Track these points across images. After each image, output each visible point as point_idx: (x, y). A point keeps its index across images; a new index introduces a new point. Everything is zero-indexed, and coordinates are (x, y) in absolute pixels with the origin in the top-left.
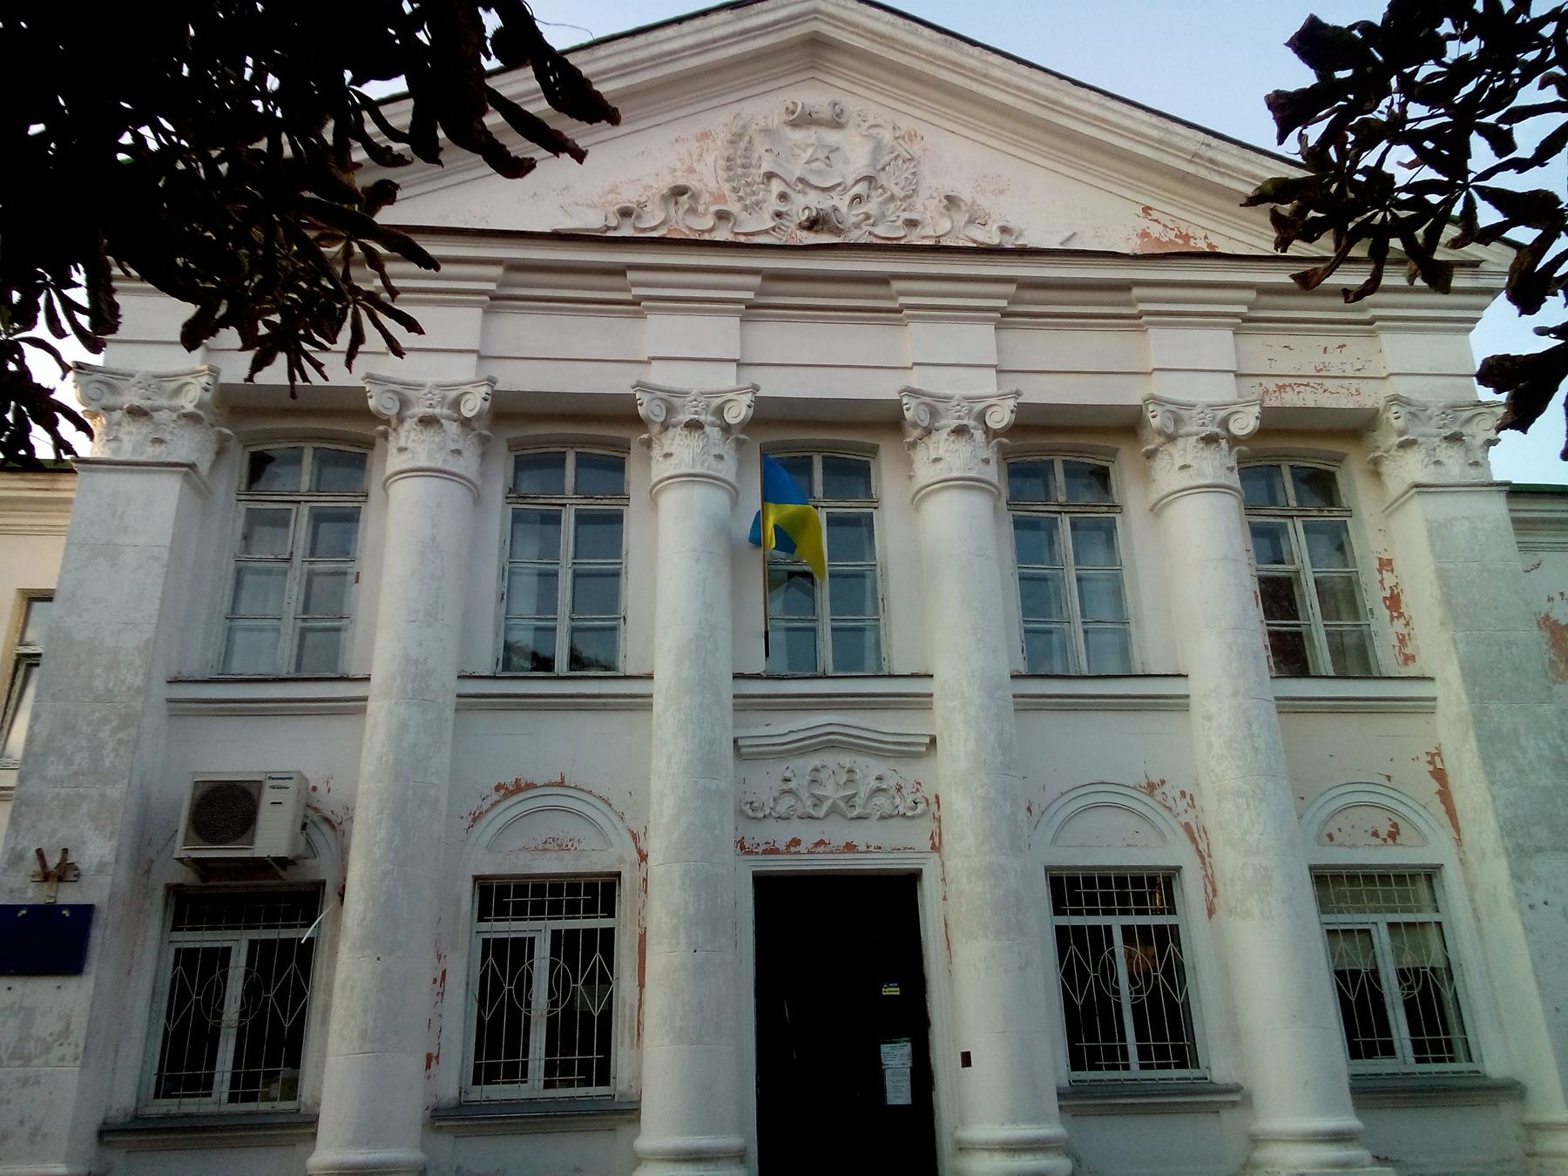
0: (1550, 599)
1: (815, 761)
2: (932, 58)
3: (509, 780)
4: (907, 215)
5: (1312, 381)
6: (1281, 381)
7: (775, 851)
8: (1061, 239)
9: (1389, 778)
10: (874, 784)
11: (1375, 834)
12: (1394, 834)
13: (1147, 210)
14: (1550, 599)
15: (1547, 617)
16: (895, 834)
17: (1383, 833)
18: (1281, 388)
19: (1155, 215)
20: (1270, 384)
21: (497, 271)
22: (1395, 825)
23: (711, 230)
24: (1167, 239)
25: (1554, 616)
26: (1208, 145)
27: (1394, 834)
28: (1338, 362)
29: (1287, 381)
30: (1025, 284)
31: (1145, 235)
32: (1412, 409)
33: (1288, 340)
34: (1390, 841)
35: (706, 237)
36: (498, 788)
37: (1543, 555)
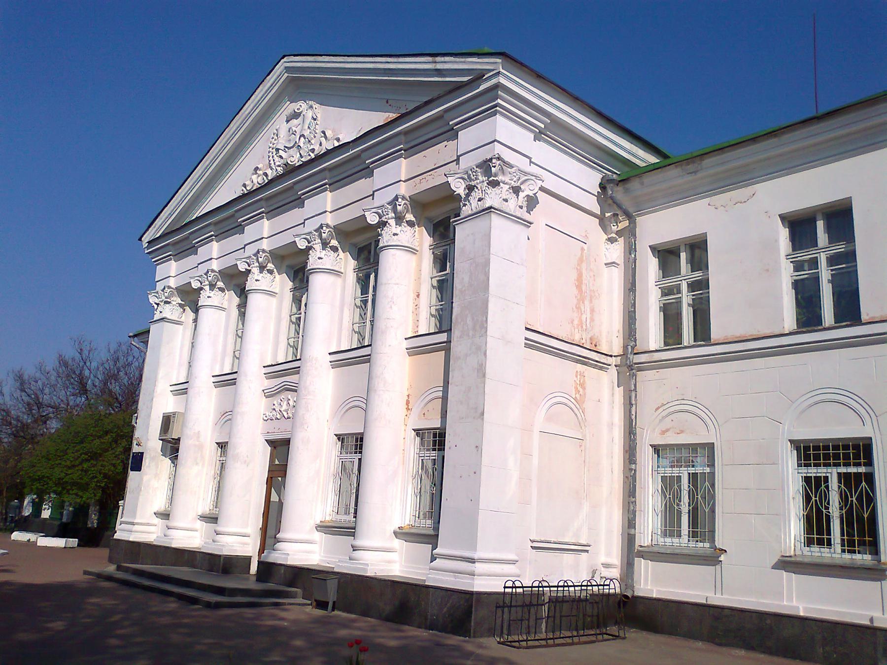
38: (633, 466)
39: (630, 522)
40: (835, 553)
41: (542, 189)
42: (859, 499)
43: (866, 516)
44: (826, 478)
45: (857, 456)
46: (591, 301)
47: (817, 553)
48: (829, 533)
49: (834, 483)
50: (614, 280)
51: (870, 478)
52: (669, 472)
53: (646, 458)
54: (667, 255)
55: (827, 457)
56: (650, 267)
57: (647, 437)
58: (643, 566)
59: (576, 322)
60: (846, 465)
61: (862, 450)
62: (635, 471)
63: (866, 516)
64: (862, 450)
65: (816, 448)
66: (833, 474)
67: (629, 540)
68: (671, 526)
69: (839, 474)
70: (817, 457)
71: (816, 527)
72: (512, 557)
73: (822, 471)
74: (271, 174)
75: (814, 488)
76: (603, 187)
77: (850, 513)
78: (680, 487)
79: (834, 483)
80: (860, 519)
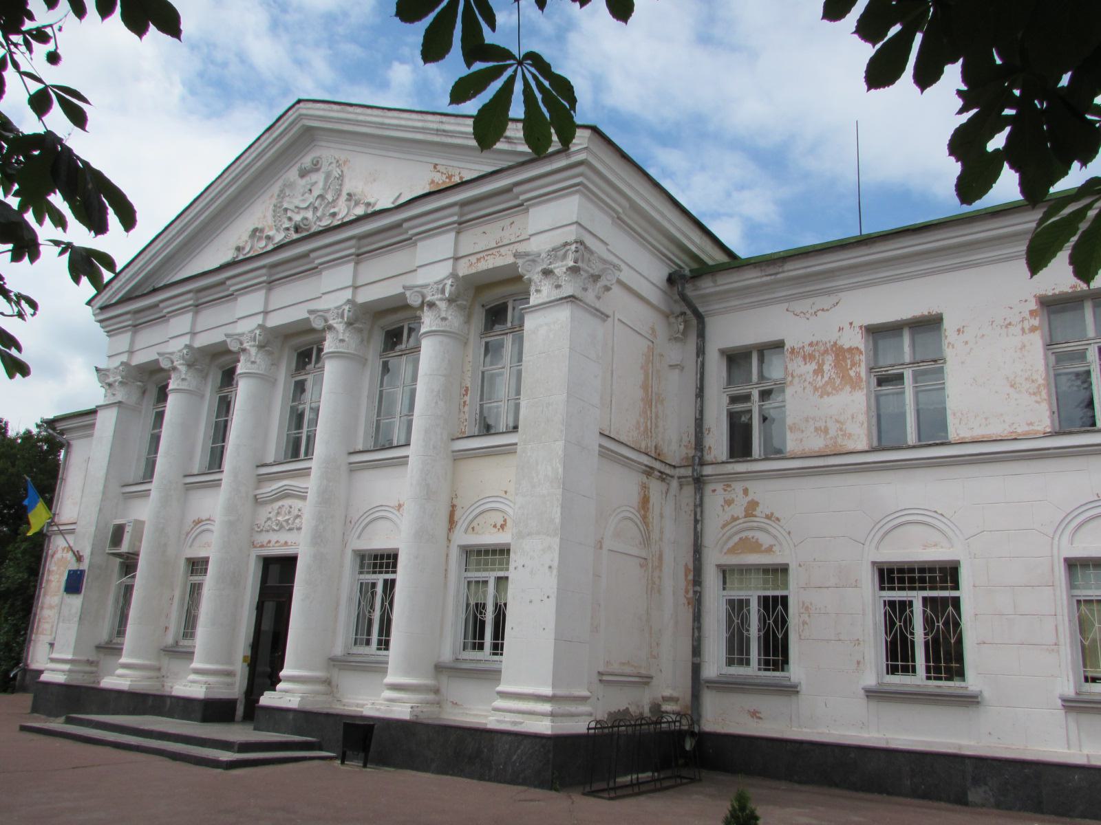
0: (841, 329)
1: (280, 503)
2: (339, 121)
3: (196, 518)
4: (332, 211)
5: (494, 251)
6: (478, 256)
7: (262, 546)
8: (392, 200)
9: (506, 492)
10: (296, 512)
11: (495, 526)
12: (502, 527)
13: (435, 166)
14: (841, 329)
15: (835, 343)
16: (283, 537)
17: (498, 526)
18: (478, 260)
19: (438, 167)
20: (473, 259)
21: (353, 242)
22: (505, 521)
23: (266, 246)
24: (441, 180)
25: (839, 343)
26: (442, 122)
27: (502, 527)
28: (509, 235)
29: (481, 255)
30: (463, 204)
31: (433, 182)
32: (530, 258)
33: (486, 228)
34: (501, 530)
35: (265, 250)
36: (194, 521)
37: (841, 295)
38: (698, 588)
39: (697, 651)
40: (918, 679)
41: (620, 282)
42: (946, 624)
43: (952, 641)
44: (911, 603)
45: (944, 580)
47: (898, 680)
48: (914, 660)
49: (918, 608)
51: (956, 602)
53: (711, 578)
54: (736, 359)
55: (912, 580)
56: (716, 369)
57: (714, 558)
61: (949, 574)
62: (700, 593)
63: (952, 641)
64: (949, 574)
65: (901, 571)
66: (916, 598)
67: (696, 669)
69: (925, 599)
70: (901, 580)
71: (898, 654)
72: (585, 693)
74: (279, 237)
75: (897, 614)
77: (936, 640)
78: (749, 611)
79: (918, 608)
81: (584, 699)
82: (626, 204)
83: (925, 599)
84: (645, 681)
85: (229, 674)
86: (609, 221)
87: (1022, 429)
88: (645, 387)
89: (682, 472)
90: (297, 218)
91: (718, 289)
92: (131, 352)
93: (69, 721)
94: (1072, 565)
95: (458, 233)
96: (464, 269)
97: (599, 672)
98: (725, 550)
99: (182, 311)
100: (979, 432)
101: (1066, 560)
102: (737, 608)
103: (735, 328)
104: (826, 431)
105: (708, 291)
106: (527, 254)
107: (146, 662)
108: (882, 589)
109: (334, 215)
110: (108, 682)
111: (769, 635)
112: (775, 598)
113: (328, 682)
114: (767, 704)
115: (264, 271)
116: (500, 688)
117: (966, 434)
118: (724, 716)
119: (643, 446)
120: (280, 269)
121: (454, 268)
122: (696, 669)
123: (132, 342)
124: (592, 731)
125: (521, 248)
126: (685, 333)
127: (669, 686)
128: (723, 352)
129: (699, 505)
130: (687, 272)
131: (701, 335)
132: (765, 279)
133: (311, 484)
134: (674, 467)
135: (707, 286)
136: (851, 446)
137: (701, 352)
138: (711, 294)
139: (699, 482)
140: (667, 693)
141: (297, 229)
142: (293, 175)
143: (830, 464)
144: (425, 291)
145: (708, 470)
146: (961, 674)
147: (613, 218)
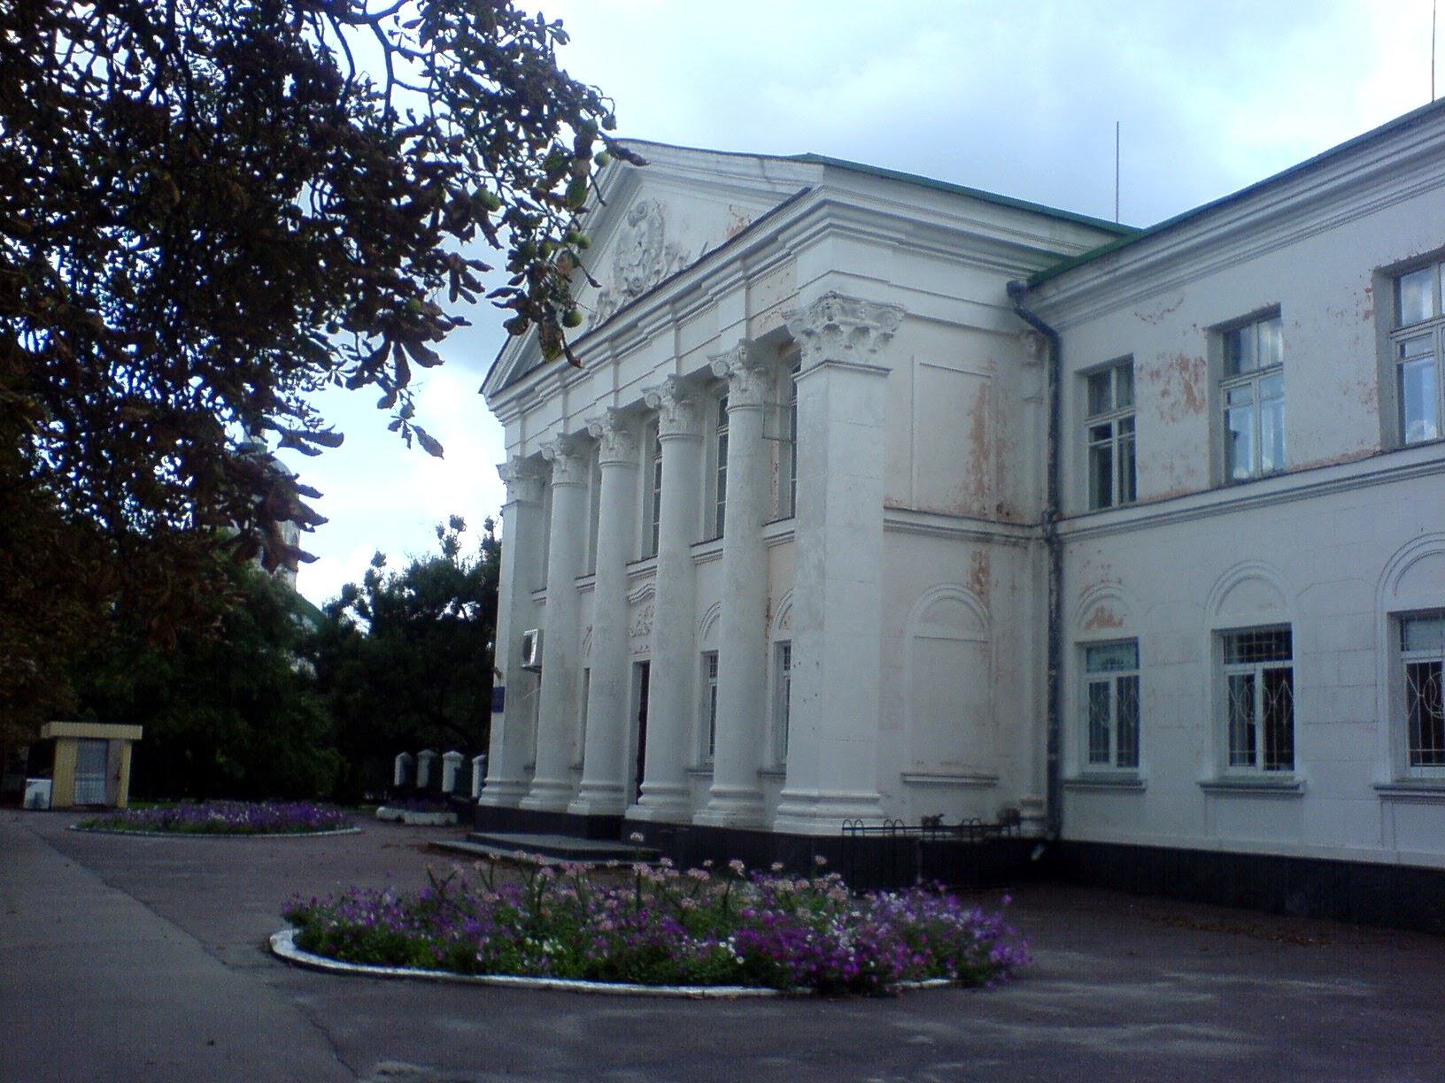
24: (737, 225)
42: (1279, 702)
46: (999, 455)
47: (1240, 772)
49: (1259, 683)
50: (1034, 421)
51: (1288, 673)
52: (1101, 677)
54: (1097, 379)
56: (1075, 395)
57: (1074, 633)
58: (1071, 802)
59: (972, 488)
60: (1269, 659)
67: (1054, 769)
68: (1098, 750)
69: (1267, 673)
73: (1248, 668)
76: (1014, 291)
80: (1280, 724)
81: (874, 801)
82: (909, 228)
83: (1267, 673)
84: (987, 783)
85: (617, 789)
86: (889, 252)
87: (1354, 449)
88: (978, 434)
89: (1039, 531)
90: (632, 277)
91: (1062, 296)
92: (523, 443)
93: (470, 839)
94: (1403, 621)
95: (749, 288)
96: (759, 332)
97: (904, 775)
98: (1083, 624)
99: (551, 396)
100: (1314, 456)
101: (1392, 615)
102: (1098, 690)
103: (1088, 345)
104: (1172, 468)
105: (1053, 301)
106: (793, 313)
107: (670, 785)
108: (1228, 661)
109: (658, 272)
110: (527, 803)
111: (1119, 725)
112: (1129, 679)
113: (684, 793)
114: (1116, 804)
115: (606, 345)
116: (787, 791)
117: (1300, 461)
118: (1094, 822)
119: (976, 507)
120: (620, 341)
121: (748, 332)
122: (1054, 769)
123: (523, 428)
124: (848, 833)
125: (785, 308)
126: (1040, 351)
127: (1023, 787)
128: (1081, 374)
129: (1058, 571)
130: (1023, 282)
131: (1056, 357)
132: (1105, 278)
133: (657, 583)
134: (1031, 527)
135: (1052, 294)
136: (1193, 485)
137: (1056, 378)
138: (1053, 306)
139: (1055, 545)
140: (1026, 796)
141: (631, 292)
142: (624, 224)
143: (1178, 509)
144: (728, 360)
145: (1062, 528)
146: (1136, 764)
147: (894, 249)
